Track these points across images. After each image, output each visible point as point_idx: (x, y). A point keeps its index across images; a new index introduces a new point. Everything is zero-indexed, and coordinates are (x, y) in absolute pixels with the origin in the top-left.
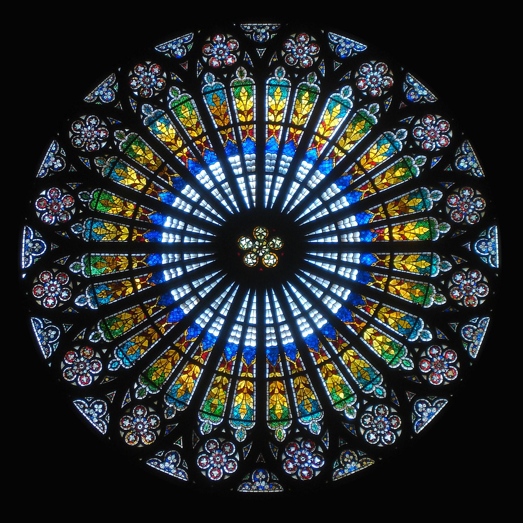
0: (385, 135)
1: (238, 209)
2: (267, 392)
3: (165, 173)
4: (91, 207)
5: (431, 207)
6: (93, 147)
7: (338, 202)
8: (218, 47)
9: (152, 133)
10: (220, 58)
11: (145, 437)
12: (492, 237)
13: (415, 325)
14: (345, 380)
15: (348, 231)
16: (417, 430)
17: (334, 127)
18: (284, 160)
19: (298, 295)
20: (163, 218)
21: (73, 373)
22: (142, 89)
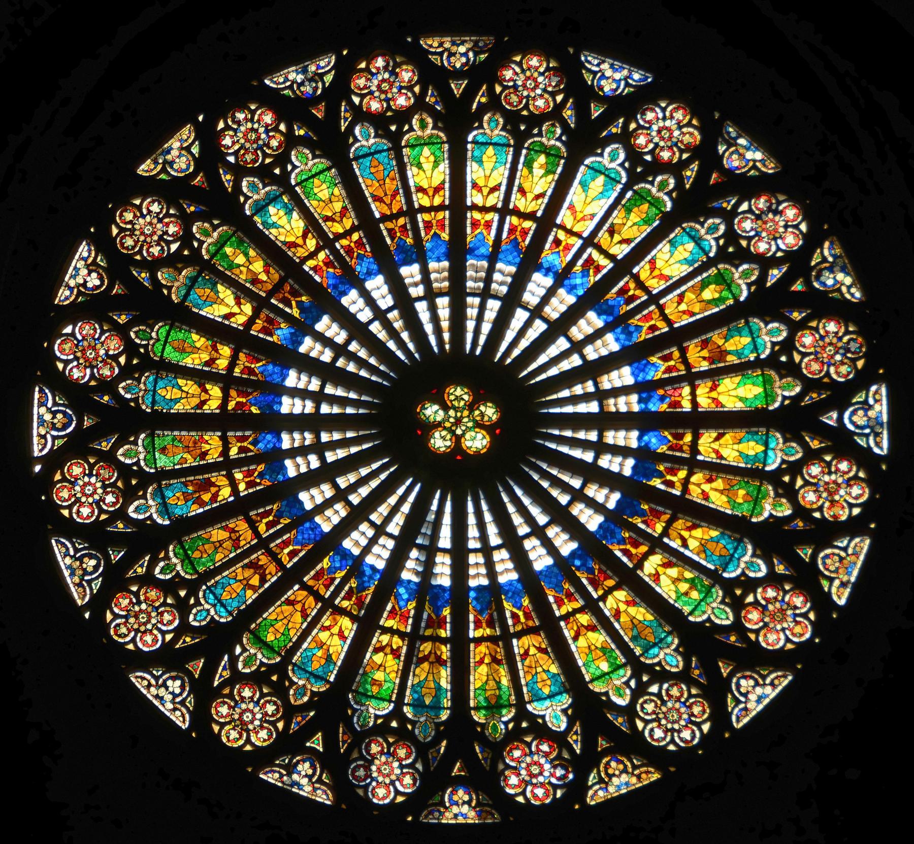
0: (684, 229)
1: (417, 355)
2: (472, 660)
3: (286, 295)
4: (154, 353)
5: (768, 352)
6: (155, 250)
7: (599, 343)
8: (380, 78)
9: (261, 227)
10: (383, 96)
11: (257, 733)
12: (876, 401)
13: (736, 549)
14: (609, 641)
15: (616, 392)
16: (738, 721)
17: (592, 216)
18: (501, 271)
19: (526, 501)
20: (282, 371)
21: (128, 629)
22: (242, 152)
